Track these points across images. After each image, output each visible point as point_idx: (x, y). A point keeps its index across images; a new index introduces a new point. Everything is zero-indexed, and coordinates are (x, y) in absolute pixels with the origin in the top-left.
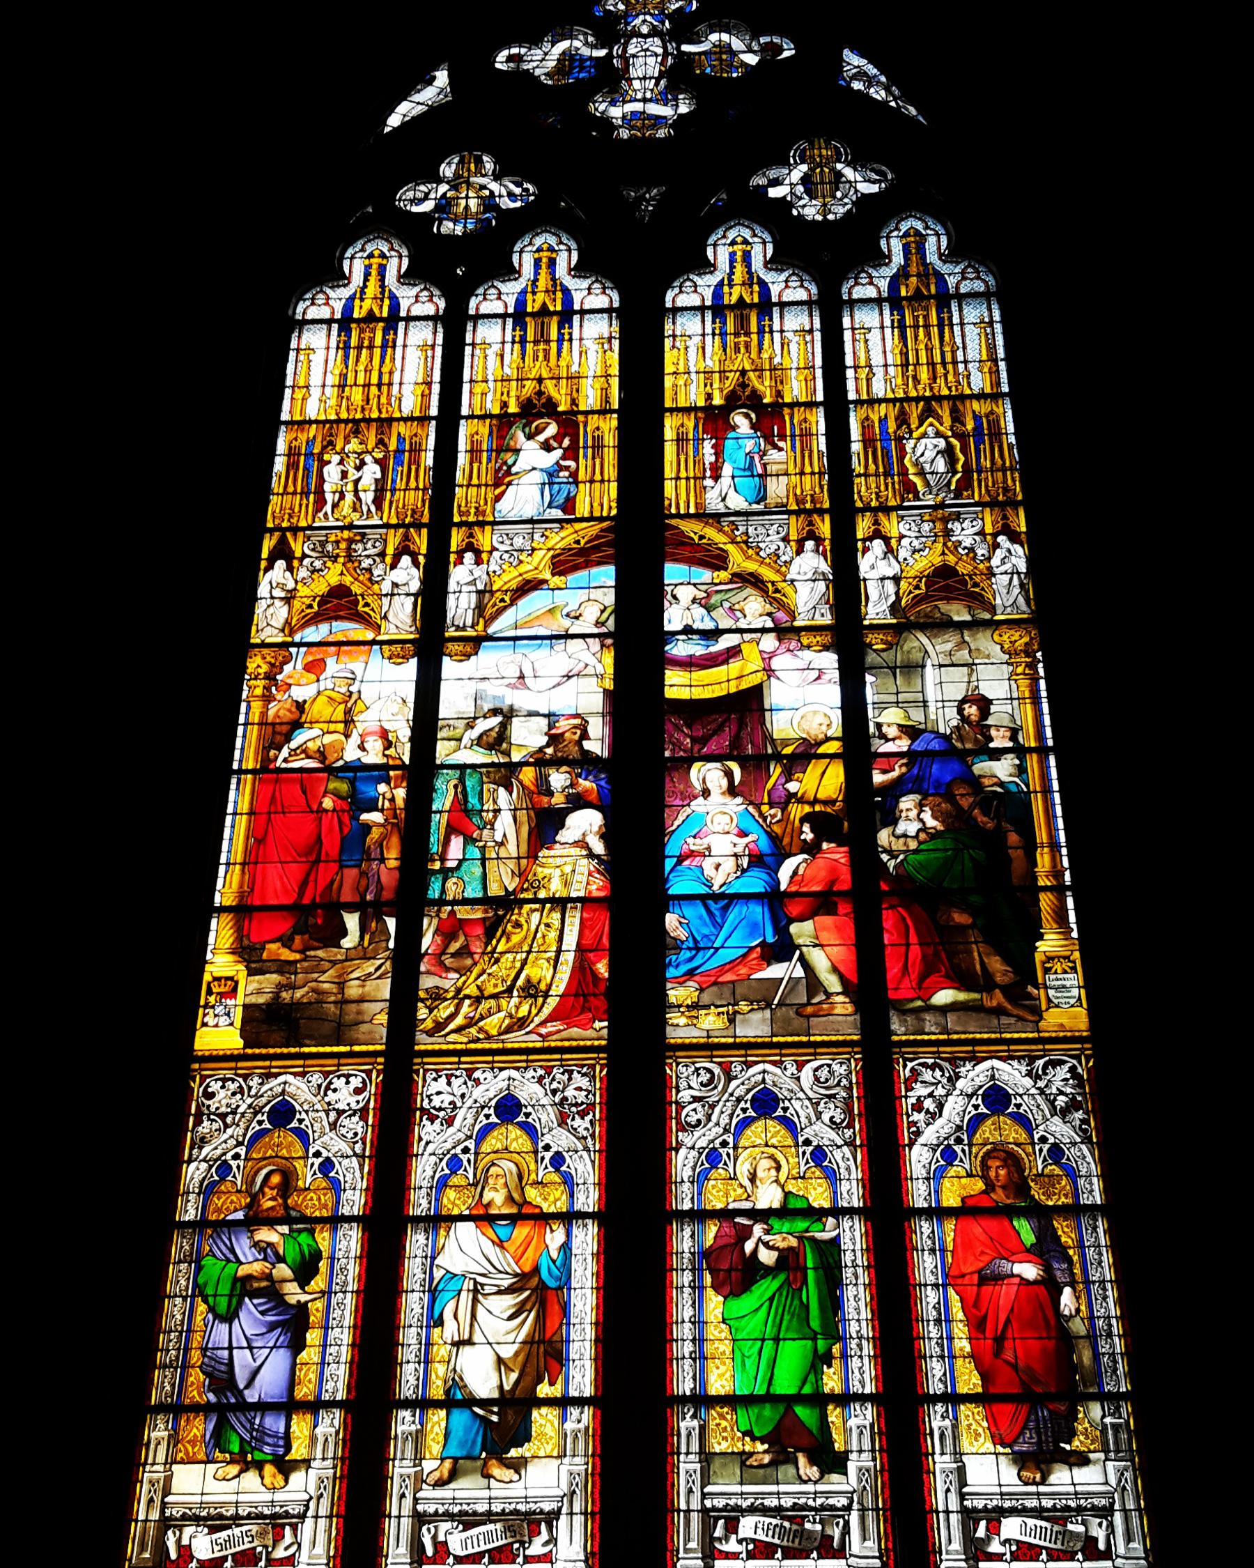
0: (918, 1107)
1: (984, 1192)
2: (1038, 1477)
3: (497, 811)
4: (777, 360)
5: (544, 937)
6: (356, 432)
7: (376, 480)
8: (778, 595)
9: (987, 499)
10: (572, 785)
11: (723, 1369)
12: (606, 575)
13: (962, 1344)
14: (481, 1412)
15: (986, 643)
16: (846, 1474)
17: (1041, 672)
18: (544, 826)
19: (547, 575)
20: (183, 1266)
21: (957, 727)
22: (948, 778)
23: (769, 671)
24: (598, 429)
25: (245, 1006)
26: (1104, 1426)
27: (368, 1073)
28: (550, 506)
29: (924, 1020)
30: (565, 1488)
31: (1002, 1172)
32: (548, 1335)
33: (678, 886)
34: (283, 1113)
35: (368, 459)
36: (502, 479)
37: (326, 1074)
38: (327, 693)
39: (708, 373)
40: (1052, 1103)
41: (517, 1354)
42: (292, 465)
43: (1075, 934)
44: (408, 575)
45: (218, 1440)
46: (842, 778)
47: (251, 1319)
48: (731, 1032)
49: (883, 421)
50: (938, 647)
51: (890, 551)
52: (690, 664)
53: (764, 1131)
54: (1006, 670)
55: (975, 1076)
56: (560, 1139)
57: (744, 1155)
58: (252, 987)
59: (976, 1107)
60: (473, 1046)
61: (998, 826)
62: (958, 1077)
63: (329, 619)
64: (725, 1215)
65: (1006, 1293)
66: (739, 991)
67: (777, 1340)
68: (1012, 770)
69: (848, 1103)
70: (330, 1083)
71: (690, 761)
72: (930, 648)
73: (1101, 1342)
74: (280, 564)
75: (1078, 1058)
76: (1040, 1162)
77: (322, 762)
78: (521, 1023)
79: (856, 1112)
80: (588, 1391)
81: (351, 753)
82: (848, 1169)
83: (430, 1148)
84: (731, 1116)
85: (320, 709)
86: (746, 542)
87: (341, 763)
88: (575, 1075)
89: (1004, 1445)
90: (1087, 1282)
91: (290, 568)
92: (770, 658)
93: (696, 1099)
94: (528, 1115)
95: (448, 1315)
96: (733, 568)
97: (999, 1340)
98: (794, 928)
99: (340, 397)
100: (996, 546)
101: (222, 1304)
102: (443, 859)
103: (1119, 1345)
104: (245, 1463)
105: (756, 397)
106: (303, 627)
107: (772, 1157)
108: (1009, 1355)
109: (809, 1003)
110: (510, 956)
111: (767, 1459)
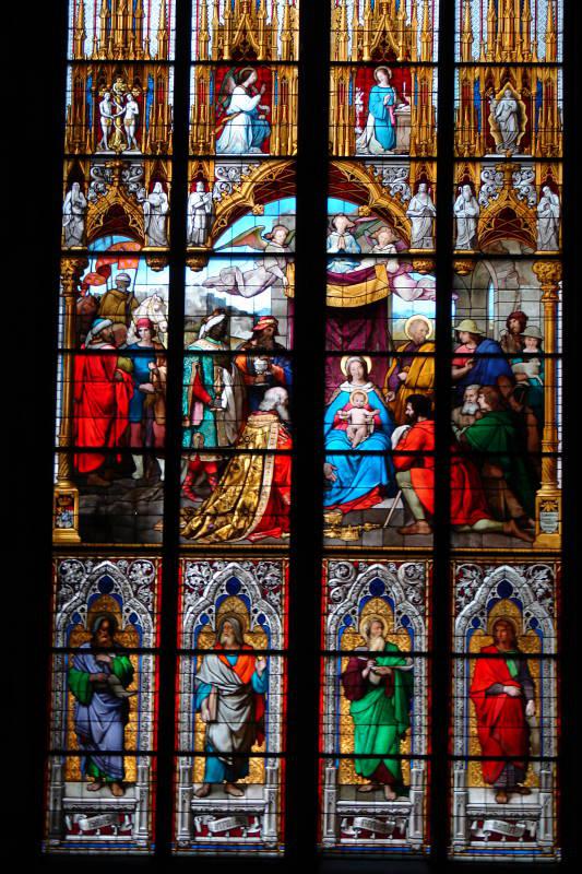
0: (462, 593)
1: (493, 645)
2: (505, 800)
3: (223, 386)
4: (408, 22)
5: (252, 475)
6: (119, 73)
7: (136, 115)
8: (400, 227)
9: (539, 155)
10: (269, 369)
11: (349, 740)
12: (289, 204)
13: (474, 730)
14: (222, 759)
15: (529, 272)
16: (408, 796)
17: (560, 296)
18: (250, 398)
19: (251, 203)
20: (60, 674)
21: (505, 336)
22: (496, 373)
23: (392, 289)
24: (284, 78)
25: (80, 516)
26: (541, 775)
27: (153, 561)
28: (253, 145)
29: (468, 539)
30: (267, 800)
31: (504, 634)
32: (258, 718)
33: (332, 445)
34: (107, 584)
35: (129, 97)
36: (220, 118)
37: (129, 561)
38: (114, 292)
39: (361, 31)
40: (535, 593)
41: (241, 728)
42: (77, 100)
43: (560, 486)
44: (159, 198)
45: (87, 769)
46: (433, 371)
47: (99, 705)
48: (359, 543)
49: (477, 82)
50: (498, 273)
51: (474, 194)
52: (344, 280)
53: (376, 606)
54: (539, 294)
55: (495, 574)
56: (262, 607)
57: (364, 619)
58: (82, 503)
59: (493, 594)
60: (212, 546)
61: (523, 409)
62: (485, 576)
63: (111, 233)
64: (352, 654)
65: (500, 702)
66: (366, 515)
67: (377, 725)
68: (536, 370)
69: (423, 591)
70: (132, 567)
71: (342, 354)
72: (493, 275)
73: (545, 730)
74: (76, 185)
75: (551, 565)
76: (524, 628)
77: (113, 345)
78: (239, 532)
79: (427, 595)
80: (279, 750)
81: (131, 339)
82: (421, 629)
83: (191, 609)
84: (358, 596)
85: (109, 303)
86: (381, 183)
87: (125, 346)
88: (271, 567)
89: (490, 783)
90: (542, 698)
91: (82, 190)
92: (393, 278)
93: (339, 584)
94: (245, 591)
95: (204, 704)
96: (372, 203)
97: (492, 728)
98: (398, 476)
99: (107, 40)
100: (542, 194)
101: (83, 697)
102: (191, 419)
103: (554, 732)
104: (101, 783)
105: (393, 54)
106: (95, 238)
107: (379, 621)
108: (497, 736)
109: (404, 527)
110: (232, 488)
111: (369, 788)
